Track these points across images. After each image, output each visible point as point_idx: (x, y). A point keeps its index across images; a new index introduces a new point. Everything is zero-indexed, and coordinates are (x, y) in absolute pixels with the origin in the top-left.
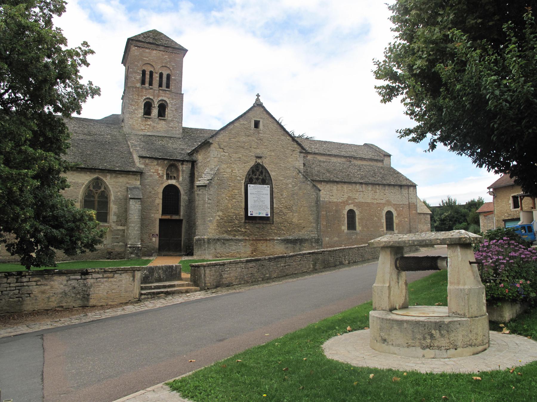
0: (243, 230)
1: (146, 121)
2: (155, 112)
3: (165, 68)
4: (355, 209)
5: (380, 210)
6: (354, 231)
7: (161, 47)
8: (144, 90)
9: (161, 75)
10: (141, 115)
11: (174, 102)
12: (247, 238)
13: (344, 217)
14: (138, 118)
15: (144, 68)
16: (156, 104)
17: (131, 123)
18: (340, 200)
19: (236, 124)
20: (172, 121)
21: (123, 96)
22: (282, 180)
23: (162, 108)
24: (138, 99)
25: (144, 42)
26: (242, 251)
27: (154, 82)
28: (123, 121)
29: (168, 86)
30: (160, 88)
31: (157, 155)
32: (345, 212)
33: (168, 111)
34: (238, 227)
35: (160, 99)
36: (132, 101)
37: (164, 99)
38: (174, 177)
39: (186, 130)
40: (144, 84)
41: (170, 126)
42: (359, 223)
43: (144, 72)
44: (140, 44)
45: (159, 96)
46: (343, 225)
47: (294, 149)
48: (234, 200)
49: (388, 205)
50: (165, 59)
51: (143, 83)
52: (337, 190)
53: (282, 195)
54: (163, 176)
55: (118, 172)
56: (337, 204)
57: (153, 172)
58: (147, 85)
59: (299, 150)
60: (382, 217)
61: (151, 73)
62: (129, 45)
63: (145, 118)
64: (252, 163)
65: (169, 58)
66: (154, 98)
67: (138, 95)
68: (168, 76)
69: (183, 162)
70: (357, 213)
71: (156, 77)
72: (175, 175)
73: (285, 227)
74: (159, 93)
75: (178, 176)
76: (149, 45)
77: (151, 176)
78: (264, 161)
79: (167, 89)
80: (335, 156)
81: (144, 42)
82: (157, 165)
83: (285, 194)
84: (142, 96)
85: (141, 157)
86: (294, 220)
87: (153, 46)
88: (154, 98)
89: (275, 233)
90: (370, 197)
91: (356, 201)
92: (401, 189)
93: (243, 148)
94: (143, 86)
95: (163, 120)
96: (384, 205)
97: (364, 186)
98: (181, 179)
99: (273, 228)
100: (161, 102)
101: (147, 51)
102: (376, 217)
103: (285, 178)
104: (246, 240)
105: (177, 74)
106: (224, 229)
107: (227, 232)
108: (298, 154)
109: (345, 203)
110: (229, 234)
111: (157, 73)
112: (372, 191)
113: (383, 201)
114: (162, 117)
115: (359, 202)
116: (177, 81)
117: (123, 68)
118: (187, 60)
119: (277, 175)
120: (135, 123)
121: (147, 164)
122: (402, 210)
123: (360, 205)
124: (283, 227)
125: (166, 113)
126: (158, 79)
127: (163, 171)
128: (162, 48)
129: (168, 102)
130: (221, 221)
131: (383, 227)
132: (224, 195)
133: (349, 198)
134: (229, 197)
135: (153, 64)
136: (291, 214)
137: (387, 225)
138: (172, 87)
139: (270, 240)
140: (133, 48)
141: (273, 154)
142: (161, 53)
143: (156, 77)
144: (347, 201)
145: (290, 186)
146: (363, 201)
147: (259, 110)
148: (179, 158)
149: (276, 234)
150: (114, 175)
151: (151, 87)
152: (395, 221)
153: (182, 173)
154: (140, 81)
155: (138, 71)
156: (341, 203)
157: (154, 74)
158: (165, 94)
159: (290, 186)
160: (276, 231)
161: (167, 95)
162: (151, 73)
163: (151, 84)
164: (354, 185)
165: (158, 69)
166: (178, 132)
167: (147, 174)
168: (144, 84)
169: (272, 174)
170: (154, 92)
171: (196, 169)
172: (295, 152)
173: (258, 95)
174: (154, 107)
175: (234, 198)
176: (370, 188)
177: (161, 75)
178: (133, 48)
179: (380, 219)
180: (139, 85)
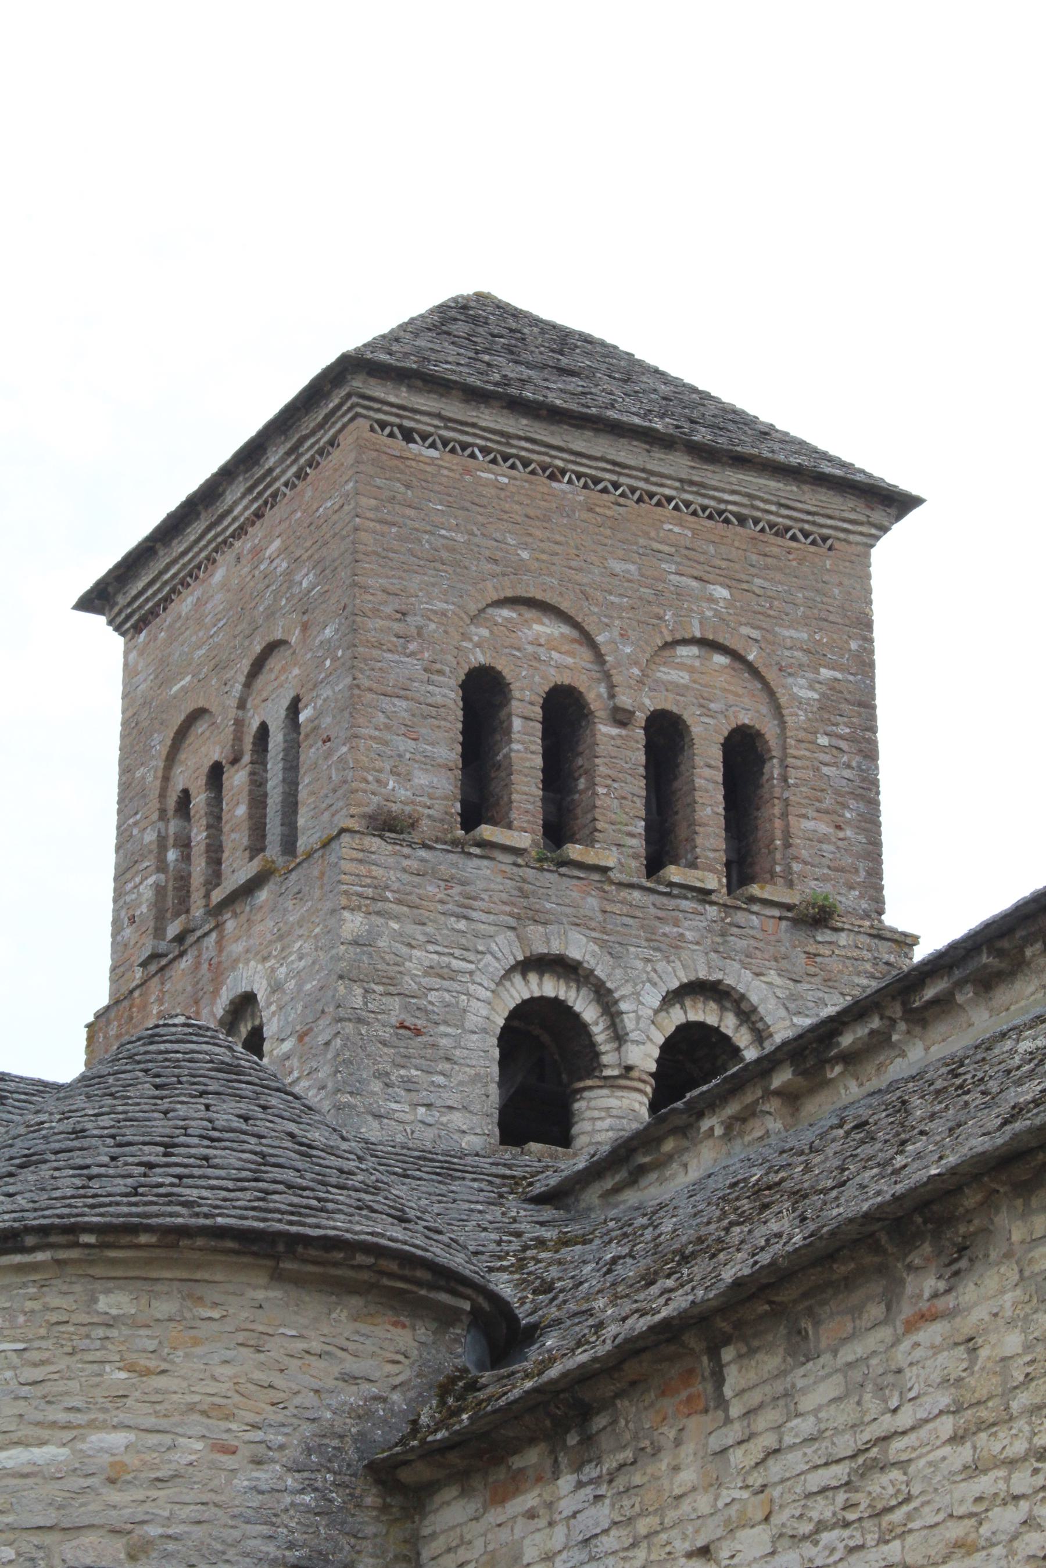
76: (178, 547)
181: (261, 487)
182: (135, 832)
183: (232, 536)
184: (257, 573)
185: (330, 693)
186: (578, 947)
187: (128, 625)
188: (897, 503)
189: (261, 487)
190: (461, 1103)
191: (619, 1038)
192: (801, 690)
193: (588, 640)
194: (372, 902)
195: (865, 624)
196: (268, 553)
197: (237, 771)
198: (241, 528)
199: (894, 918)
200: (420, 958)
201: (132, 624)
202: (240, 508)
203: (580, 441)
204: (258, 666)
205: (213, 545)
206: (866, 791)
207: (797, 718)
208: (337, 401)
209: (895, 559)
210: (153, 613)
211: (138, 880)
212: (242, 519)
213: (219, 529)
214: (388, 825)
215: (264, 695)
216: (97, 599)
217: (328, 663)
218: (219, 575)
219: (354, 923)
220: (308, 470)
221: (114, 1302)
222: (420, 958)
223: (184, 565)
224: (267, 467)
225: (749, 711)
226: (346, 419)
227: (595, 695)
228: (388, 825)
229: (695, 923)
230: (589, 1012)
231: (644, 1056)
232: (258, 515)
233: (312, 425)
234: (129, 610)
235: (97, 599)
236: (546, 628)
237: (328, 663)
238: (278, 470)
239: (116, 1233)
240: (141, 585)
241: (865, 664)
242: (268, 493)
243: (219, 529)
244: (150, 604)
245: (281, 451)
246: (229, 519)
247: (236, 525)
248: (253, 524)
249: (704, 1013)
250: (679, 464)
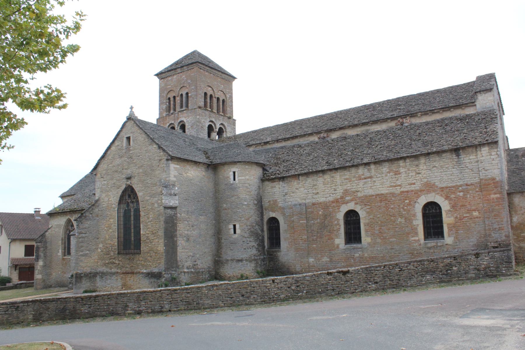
0: (117, 262)
4: (358, 209)
5: (409, 204)
6: (359, 246)
7: (178, 70)
12: (119, 271)
13: (338, 224)
15: (169, 96)
18: (331, 199)
19: (113, 148)
22: (147, 201)
26: (115, 286)
32: (341, 216)
34: (114, 259)
35: (179, 121)
42: (366, 231)
45: (178, 118)
46: (337, 236)
47: (160, 158)
48: (111, 230)
49: (429, 192)
52: (324, 184)
53: (148, 218)
56: (325, 206)
59: (166, 158)
60: (414, 215)
64: (124, 187)
70: (362, 214)
73: (151, 256)
76: (169, 73)
78: (132, 182)
80: (375, 122)
83: (151, 216)
84: (166, 124)
86: (159, 248)
87: (172, 72)
89: (142, 265)
90: (388, 184)
91: (359, 195)
92: (458, 155)
93: (116, 171)
96: (418, 193)
97: (372, 166)
99: (141, 259)
100: (181, 124)
101: (170, 78)
102: (401, 216)
103: (151, 196)
104: (117, 273)
106: (103, 262)
107: (105, 265)
108: (165, 162)
109: (339, 202)
110: (107, 267)
112: (389, 172)
113: (417, 186)
115: (366, 196)
119: (144, 194)
122: (464, 197)
123: (366, 201)
124: (149, 258)
128: (179, 70)
130: (102, 253)
131: (416, 234)
132: (103, 226)
133: (346, 192)
134: (107, 227)
136: (157, 240)
137: (425, 228)
139: (136, 273)
141: (141, 170)
142: (180, 75)
144: (342, 198)
145: (156, 205)
146: (371, 192)
147: (131, 123)
149: (143, 266)
152: (447, 220)
156: (333, 202)
159: (156, 205)
160: (143, 263)
164: (353, 170)
169: (140, 194)
172: (162, 162)
173: (132, 108)
175: (110, 228)
176: (385, 168)
179: (409, 220)
186: (213, 120)
188: (234, 78)
190: (204, 134)
191: (216, 128)
192: (228, 96)
193: (213, 90)
194: (199, 115)
195: (232, 90)
199: (234, 118)
200: (203, 120)
201: (161, 79)
203: (213, 71)
204: (181, 88)
206: (232, 106)
207: (228, 98)
209: (235, 83)
214: (200, 107)
216: (157, 75)
218: (175, 77)
219: (198, 117)
221: (247, 167)
222: (203, 120)
225: (224, 98)
227: (213, 95)
228: (200, 107)
229: (221, 118)
230: (213, 126)
231: (217, 130)
235: (157, 75)
236: (210, 89)
239: (248, 162)
241: (232, 94)
249: (221, 126)
250: (220, 73)
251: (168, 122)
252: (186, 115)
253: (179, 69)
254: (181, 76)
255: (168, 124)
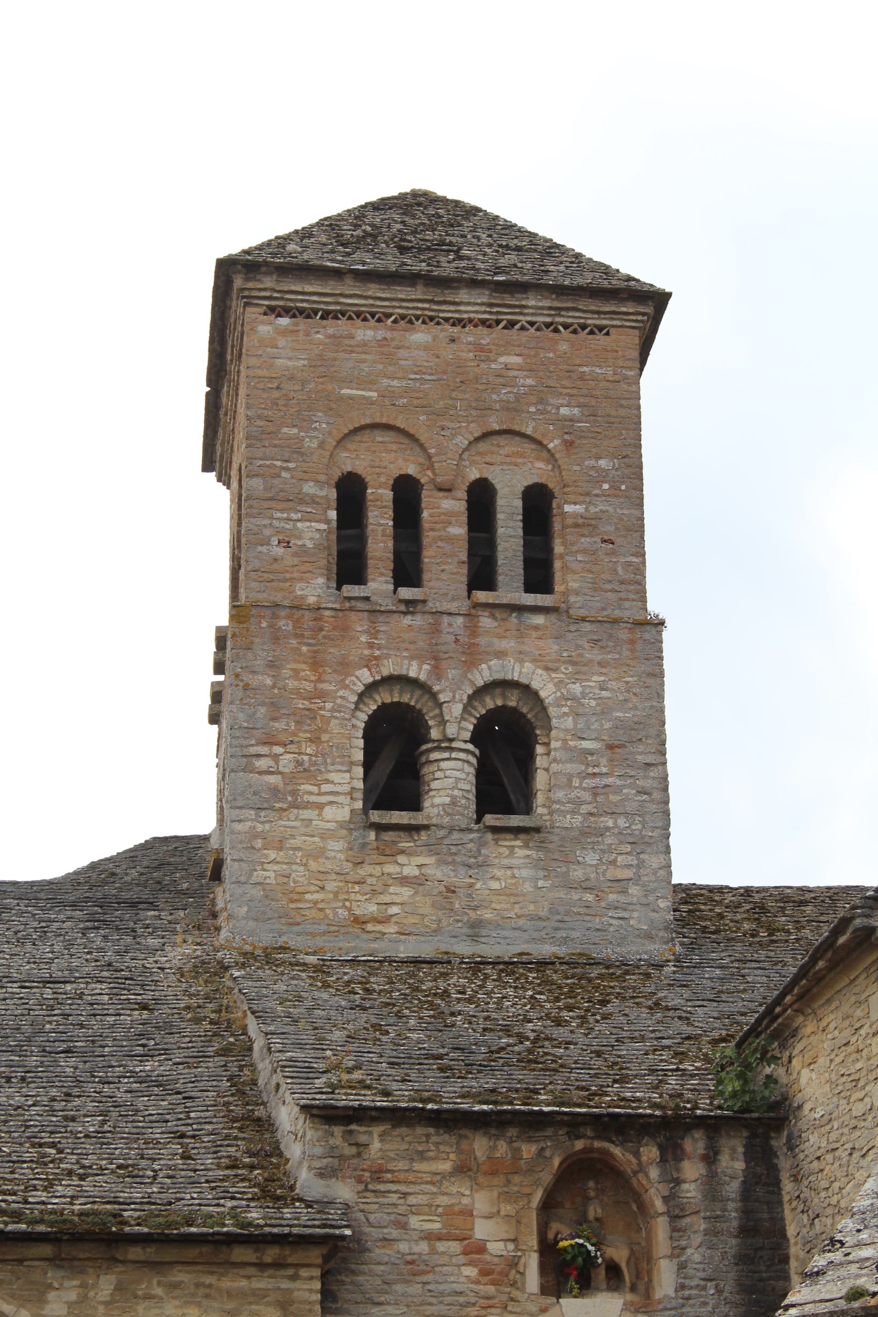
1: (389, 853)
2: (450, 780)
3: (510, 446)
7: (463, 295)
8: (359, 624)
9: (481, 500)
10: (344, 814)
11: (591, 687)
14: (325, 835)
15: (353, 460)
16: (454, 721)
17: (270, 875)
20: (589, 834)
21: (217, 696)
23: (507, 744)
24: (322, 695)
25: (338, 274)
27: (429, 555)
28: (217, 875)
29: (539, 575)
30: (481, 596)
31: (452, 1095)
33: (550, 767)
35: (483, 675)
36: (275, 709)
37: (519, 671)
38: (613, 1270)
39: (699, 908)
40: (359, 579)
41: (577, 873)
43: (351, 494)
44: (310, 290)
45: (472, 656)
50: (504, 376)
51: (350, 567)
54: (513, 1263)
55: (135, 1253)
57: (430, 1237)
58: (379, 584)
61: (407, 494)
62: (236, 305)
63: (380, 828)
65: (531, 370)
66: (437, 671)
67: (316, 664)
68: (538, 505)
69: (669, 1129)
71: (445, 520)
72: (619, 1253)
74: (473, 630)
75: (642, 1261)
76: (373, 290)
77: (414, 1268)
79: (530, 599)
81: (338, 274)
82: (462, 1170)
84: (344, 667)
85: (325, 1115)
87: (402, 292)
88: (437, 671)
94: (351, 590)
95: (517, 831)
98: (665, 1281)
100: (490, 703)
101: (366, 333)
105: (603, 475)
111: (446, 489)
114: (509, 810)
116: (608, 529)
117: (215, 500)
118: (667, 384)
120: (299, 873)
121: (378, 1173)
125: (541, 780)
126: (459, 530)
127: (517, 1220)
128: (472, 303)
129: (547, 692)
135: (418, 424)
138: (570, 577)
140: (262, 330)
142: (469, 335)
143: (445, 520)
148: (641, 1096)
150: (105, 1285)
151: (405, 593)
153: (676, 1230)
154: (327, 560)
155: (309, 488)
157: (428, 498)
158: (520, 636)
161: (531, 644)
162: (407, 494)
163: (407, 571)
165: (451, 459)
166: (638, 920)
167: (379, 1253)
168: (359, 579)
170: (435, 630)
171: (788, 1187)
174: (446, 744)
177: (481, 500)
178: (262, 330)
180: (316, 588)
181: (506, 310)
182: (283, 474)
183: (447, 320)
184: (483, 366)
185: (610, 509)
187: (266, 303)
189: (506, 310)
196: (503, 359)
197: (447, 498)
198: (460, 321)
202: (469, 308)
204: (486, 435)
205: (419, 312)
208: (631, 310)
210: (308, 314)
211: (294, 516)
212: (466, 316)
213: (435, 307)
215: (488, 459)
217: (606, 486)
220: (561, 328)
223: (372, 305)
224: (524, 303)
226: (628, 324)
232: (483, 322)
233: (593, 308)
234: (276, 295)
237: (606, 486)
238: (531, 311)
240: (309, 288)
242: (509, 317)
243: (435, 307)
244: (305, 305)
245: (546, 303)
246: (452, 308)
247: (457, 316)
248: (475, 326)
251: (369, 663)
252: (552, 648)
253: (483, 296)
254: (483, 353)
255: (366, 676)
